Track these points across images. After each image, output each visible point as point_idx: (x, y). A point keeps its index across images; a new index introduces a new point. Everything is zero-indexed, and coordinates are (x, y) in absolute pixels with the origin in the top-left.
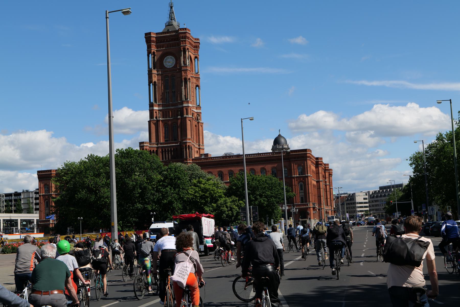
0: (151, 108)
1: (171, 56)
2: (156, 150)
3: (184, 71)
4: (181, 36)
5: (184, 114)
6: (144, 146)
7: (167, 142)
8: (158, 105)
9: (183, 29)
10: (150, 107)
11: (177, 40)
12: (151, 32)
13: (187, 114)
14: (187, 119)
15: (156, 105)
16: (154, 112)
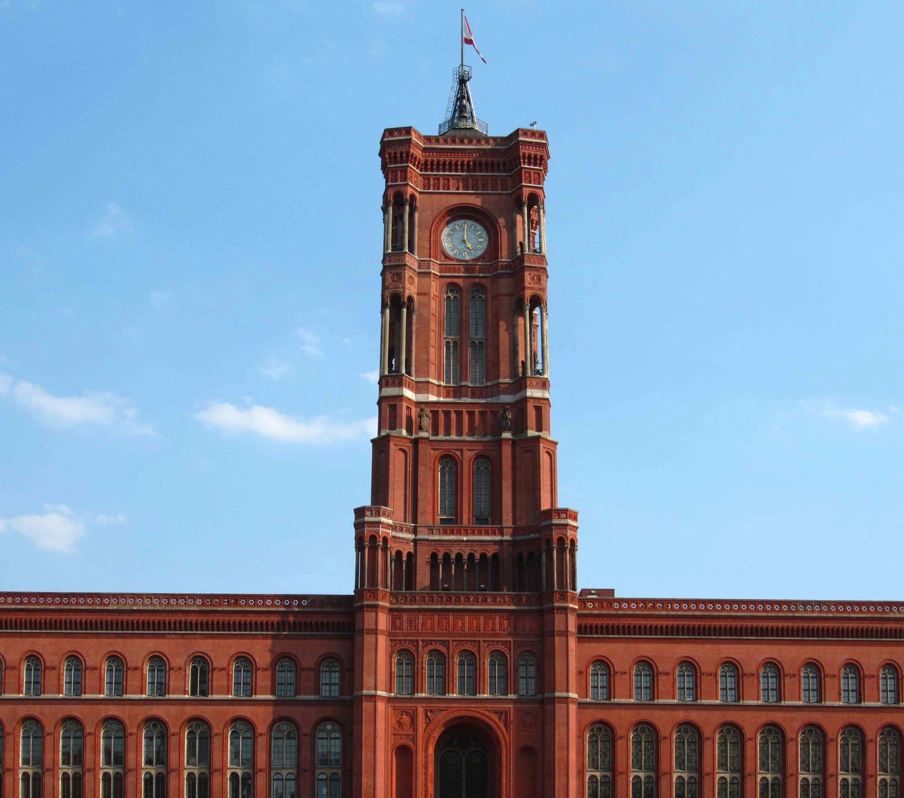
0: (390, 391)
1: (470, 223)
2: (409, 554)
3: (533, 273)
4: (524, 155)
5: (529, 424)
6: (379, 523)
7: (452, 523)
8: (416, 382)
9: (533, 134)
10: (384, 382)
11: (502, 167)
12: (411, 127)
13: (539, 428)
14: (541, 445)
15: (409, 385)
16: (405, 404)
